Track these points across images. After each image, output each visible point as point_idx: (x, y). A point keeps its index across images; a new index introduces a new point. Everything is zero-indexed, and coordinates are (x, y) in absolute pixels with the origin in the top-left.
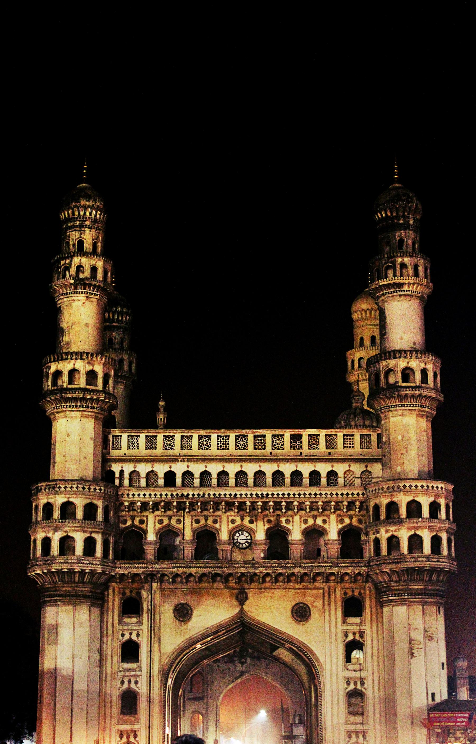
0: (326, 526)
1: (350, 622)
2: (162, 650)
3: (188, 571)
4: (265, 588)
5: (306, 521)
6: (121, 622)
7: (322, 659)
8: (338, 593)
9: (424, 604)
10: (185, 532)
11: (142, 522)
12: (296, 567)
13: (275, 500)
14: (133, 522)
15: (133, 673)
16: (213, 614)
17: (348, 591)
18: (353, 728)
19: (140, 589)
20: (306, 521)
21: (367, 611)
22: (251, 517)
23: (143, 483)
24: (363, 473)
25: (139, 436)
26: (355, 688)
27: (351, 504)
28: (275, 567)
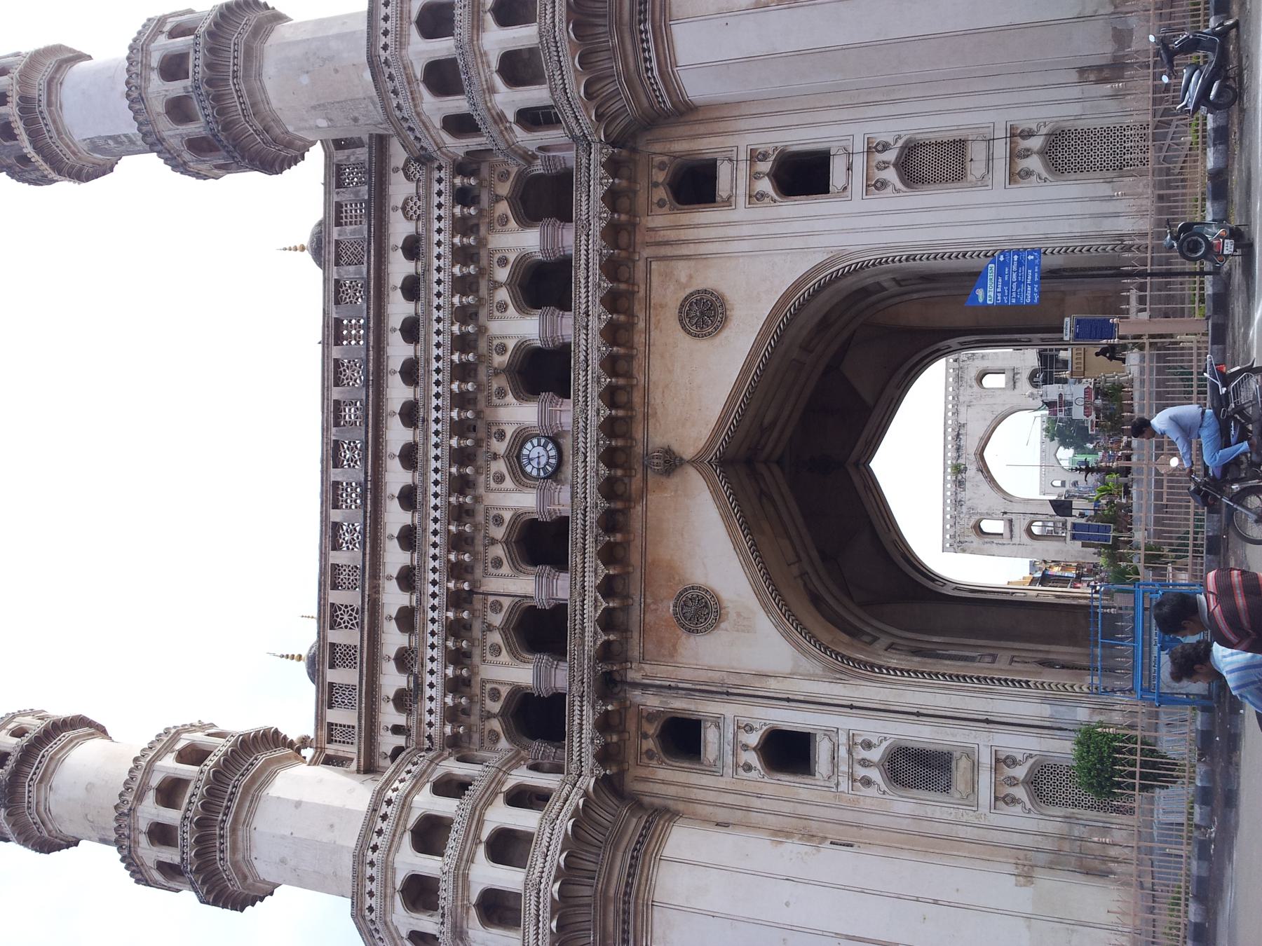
0: (512, 257)
1: (728, 187)
3: (591, 593)
4: (646, 403)
5: (503, 307)
7: (819, 258)
10: (520, 592)
11: (495, 695)
12: (586, 328)
13: (447, 378)
14: (494, 716)
15: (843, 752)
17: (655, 201)
18: (1001, 166)
19: (640, 713)
20: (503, 307)
21: (706, 146)
22: (489, 437)
24: (408, 177)
25: (331, 685)
26: (895, 165)
27: (463, 197)
28: (588, 375)
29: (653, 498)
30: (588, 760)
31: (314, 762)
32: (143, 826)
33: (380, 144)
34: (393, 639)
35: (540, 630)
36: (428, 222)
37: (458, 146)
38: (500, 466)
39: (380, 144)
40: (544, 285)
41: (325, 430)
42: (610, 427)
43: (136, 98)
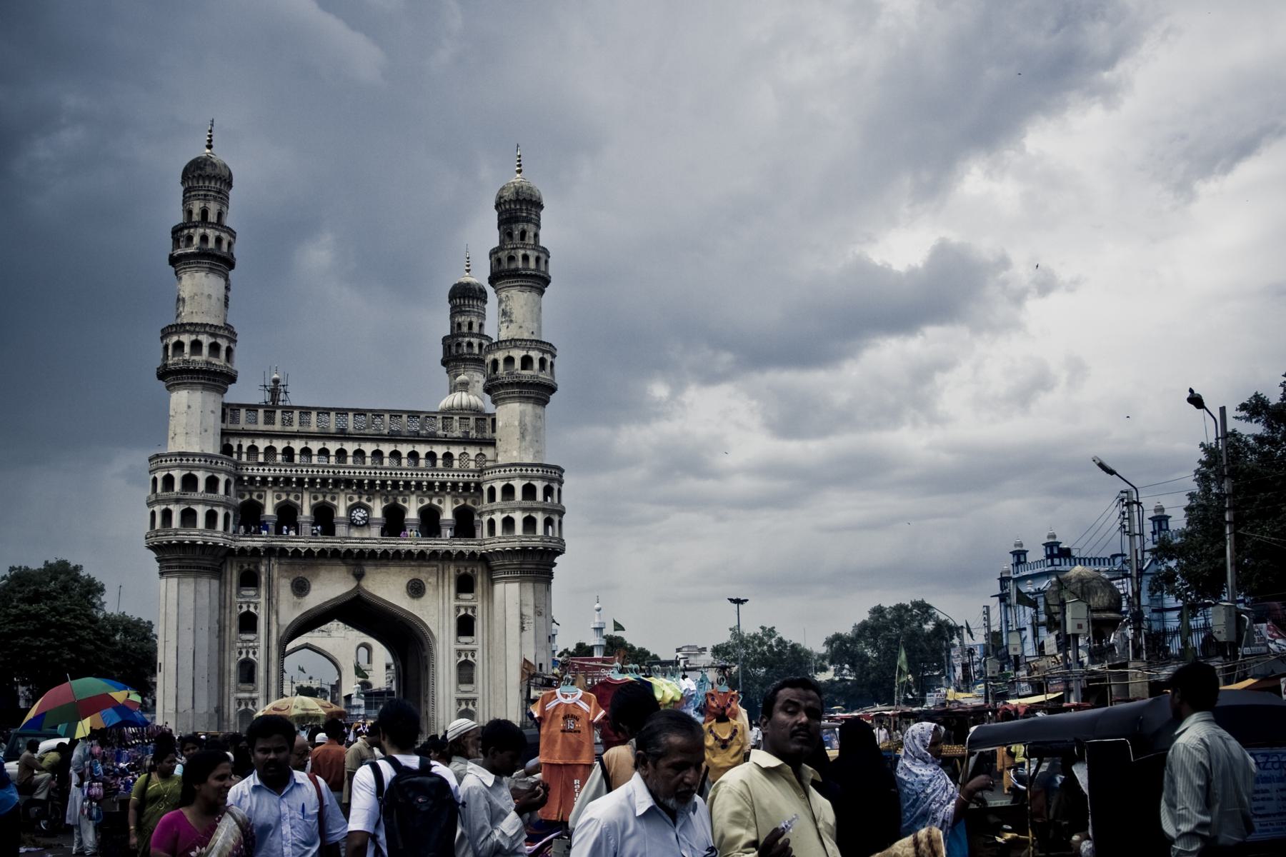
2: (281, 622)
4: (382, 565)
5: (422, 501)
6: (238, 593)
7: (435, 633)
8: (452, 570)
9: (535, 581)
11: (260, 497)
16: (329, 587)
20: (422, 501)
23: (261, 459)
27: (467, 486)
29: (344, 568)
30: (240, 544)
31: (223, 404)
32: (201, 337)
33: (492, 443)
34: (280, 445)
35: (288, 515)
36: (456, 470)
37: (485, 487)
38: (356, 499)
39: (492, 443)
40: (430, 522)
41: (371, 411)
42: (373, 552)
43: (514, 343)
